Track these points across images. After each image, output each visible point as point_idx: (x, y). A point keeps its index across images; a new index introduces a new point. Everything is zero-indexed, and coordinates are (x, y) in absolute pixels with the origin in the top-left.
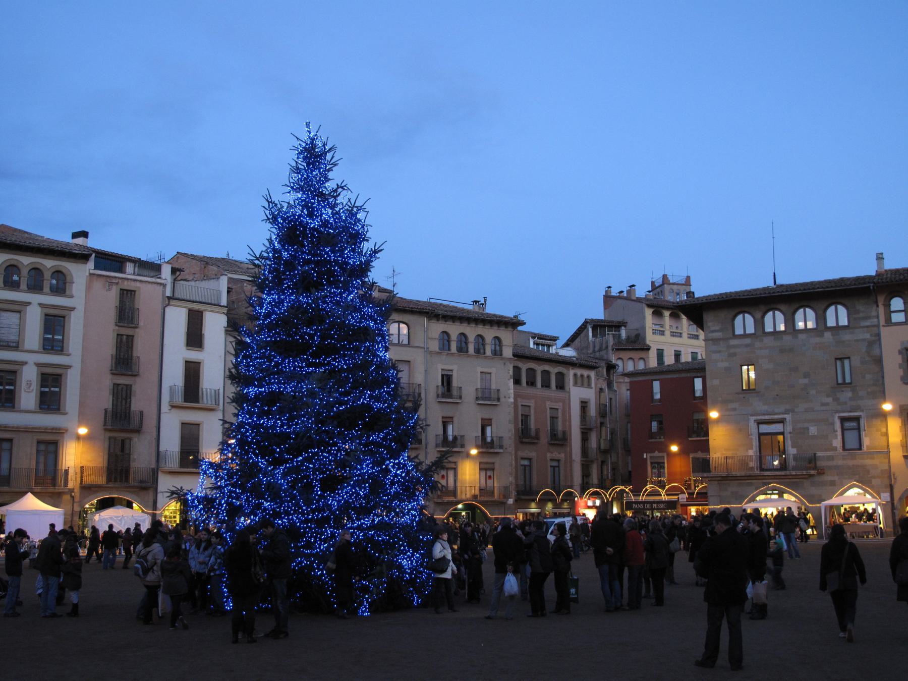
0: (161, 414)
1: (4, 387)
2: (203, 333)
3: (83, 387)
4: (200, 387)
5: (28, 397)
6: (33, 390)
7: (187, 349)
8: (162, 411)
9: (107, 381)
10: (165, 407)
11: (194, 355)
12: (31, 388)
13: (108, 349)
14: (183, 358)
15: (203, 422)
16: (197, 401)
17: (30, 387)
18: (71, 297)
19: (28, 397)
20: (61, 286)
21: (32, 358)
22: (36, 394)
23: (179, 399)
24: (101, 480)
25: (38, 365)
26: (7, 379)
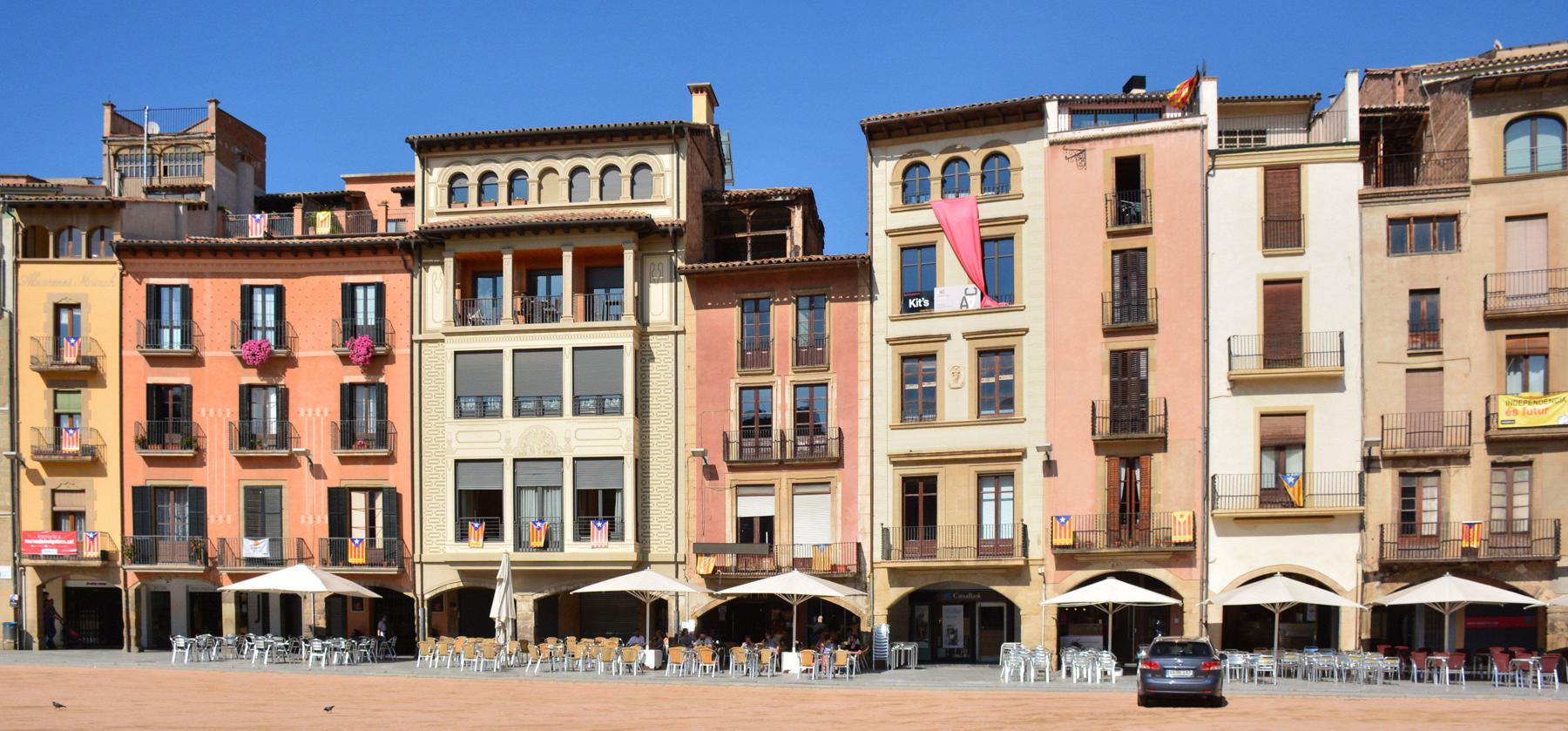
0: (1210, 401)
1: (920, 385)
2: (1302, 212)
3: (1052, 366)
4: (1304, 331)
5: (956, 397)
6: (963, 383)
7: (1266, 256)
8: (1211, 397)
9: (1099, 351)
10: (1219, 384)
11: (1283, 267)
12: (960, 381)
13: (1097, 281)
14: (1258, 276)
15: (1312, 407)
16: (1297, 361)
17: (957, 379)
18: (1020, 196)
19: (956, 397)
20: (998, 180)
21: (955, 327)
22: (970, 389)
23: (1252, 365)
24: (1100, 542)
25: (968, 336)
26: (924, 370)
